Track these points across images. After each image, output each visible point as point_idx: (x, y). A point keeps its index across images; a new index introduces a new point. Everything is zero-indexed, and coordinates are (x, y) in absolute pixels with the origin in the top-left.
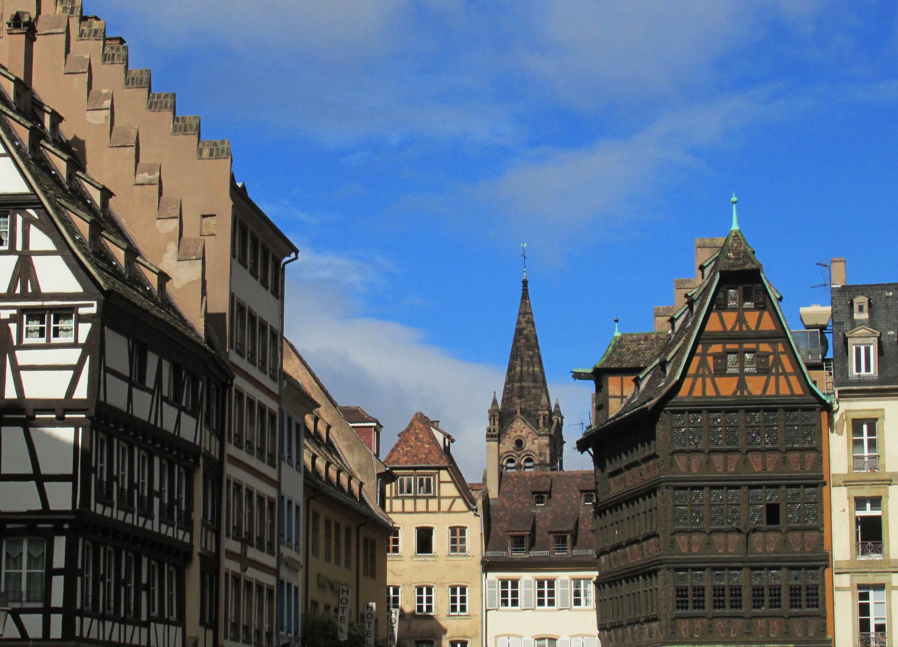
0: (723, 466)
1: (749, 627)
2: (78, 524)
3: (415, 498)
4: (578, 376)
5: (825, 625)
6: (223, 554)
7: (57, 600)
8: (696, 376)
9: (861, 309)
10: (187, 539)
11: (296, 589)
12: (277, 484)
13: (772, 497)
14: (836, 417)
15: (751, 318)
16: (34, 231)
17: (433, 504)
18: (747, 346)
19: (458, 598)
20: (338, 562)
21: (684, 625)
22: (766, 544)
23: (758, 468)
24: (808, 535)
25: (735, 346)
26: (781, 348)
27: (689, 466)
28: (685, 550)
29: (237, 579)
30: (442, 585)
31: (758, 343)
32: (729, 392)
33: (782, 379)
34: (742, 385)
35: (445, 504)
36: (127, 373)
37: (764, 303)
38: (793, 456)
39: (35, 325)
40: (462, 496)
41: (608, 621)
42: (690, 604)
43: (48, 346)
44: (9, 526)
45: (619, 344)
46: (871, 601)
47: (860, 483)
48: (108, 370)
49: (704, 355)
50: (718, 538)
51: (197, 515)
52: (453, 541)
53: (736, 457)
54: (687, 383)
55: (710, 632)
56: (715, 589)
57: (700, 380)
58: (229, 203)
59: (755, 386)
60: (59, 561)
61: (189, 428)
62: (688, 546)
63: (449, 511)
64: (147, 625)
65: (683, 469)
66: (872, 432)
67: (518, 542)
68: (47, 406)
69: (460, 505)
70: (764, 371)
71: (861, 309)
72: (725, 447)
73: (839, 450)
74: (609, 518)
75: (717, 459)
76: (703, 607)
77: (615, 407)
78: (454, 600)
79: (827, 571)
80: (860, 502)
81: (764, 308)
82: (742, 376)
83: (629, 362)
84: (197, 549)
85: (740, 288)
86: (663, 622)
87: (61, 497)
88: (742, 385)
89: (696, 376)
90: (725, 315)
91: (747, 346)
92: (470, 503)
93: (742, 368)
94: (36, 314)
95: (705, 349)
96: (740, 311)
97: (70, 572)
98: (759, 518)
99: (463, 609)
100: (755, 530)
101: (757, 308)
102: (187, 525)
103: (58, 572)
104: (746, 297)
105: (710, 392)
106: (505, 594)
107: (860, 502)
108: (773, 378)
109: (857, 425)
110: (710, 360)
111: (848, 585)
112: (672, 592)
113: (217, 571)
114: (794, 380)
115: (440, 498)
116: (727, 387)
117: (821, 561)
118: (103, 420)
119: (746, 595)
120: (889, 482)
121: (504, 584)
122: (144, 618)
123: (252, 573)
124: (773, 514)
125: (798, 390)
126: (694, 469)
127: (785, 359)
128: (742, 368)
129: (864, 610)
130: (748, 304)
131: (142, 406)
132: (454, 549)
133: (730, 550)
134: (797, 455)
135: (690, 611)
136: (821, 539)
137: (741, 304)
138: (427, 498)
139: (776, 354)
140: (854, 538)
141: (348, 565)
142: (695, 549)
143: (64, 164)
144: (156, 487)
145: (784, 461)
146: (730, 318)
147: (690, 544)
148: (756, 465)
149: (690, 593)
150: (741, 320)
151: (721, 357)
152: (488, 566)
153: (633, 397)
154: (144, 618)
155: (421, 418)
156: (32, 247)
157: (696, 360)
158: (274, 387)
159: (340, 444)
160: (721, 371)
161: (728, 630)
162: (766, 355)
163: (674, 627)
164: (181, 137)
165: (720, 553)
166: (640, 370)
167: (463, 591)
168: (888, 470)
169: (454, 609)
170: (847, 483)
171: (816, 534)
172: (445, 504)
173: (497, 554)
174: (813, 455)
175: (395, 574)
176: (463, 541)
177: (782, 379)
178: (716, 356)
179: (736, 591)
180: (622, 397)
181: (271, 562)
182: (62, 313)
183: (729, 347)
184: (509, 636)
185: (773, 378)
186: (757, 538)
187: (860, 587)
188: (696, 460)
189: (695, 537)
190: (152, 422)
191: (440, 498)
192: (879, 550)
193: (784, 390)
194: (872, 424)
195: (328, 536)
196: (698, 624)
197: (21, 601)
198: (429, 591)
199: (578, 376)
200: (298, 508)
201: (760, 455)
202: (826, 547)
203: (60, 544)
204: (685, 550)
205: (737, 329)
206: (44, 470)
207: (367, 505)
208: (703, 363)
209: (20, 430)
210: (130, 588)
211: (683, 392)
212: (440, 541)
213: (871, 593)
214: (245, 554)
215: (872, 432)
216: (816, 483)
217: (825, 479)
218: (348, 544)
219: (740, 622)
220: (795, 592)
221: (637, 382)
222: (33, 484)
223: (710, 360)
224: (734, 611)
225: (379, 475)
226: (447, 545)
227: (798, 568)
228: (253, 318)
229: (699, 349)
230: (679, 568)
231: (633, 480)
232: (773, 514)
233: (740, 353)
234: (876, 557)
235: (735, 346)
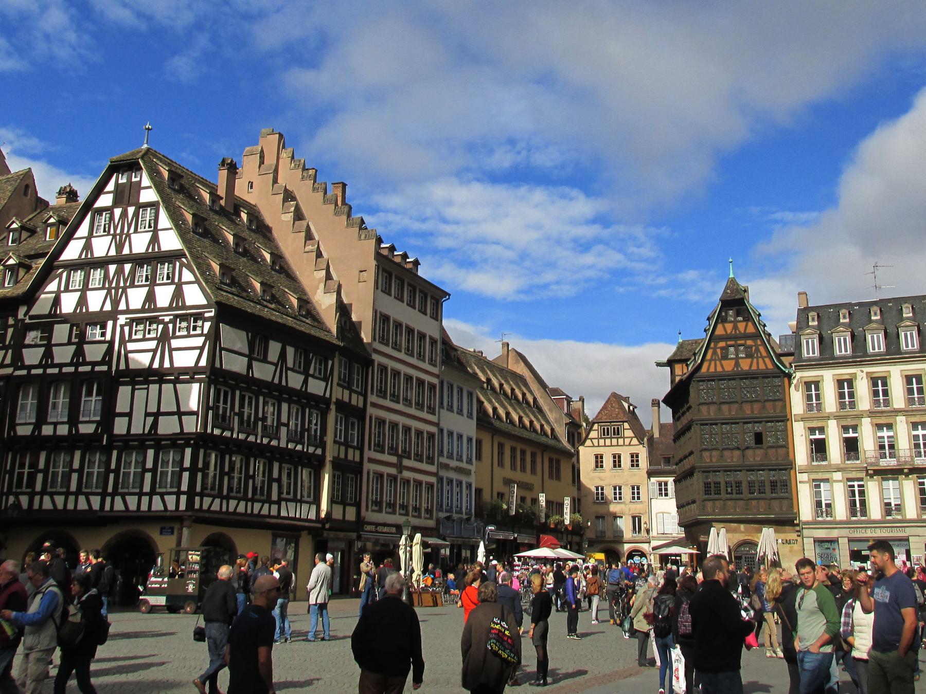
0: (727, 411)
2: (201, 441)
3: (611, 438)
4: (659, 364)
6: (365, 460)
7: (184, 487)
9: (813, 320)
10: (319, 451)
11: (469, 486)
12: (437, 425)
13: (758, 428)
14: (795, 381)
16: (184, 270)
17: (621, 441)
18: (739, 342)
19: (636, 491)
20: (523, 469)
21: (709, 504)
22: (755, 456)
23: (748, 412)
24: (779, 450)
25: (733, 343)
26: (759, 342)
27: (709, 412)
28: (708, 460)
29: (393, 478)
30: (627, 485)
32: (730, 369)
33: (760, 360)
34: (737, 364)
35: (627, 441)
37: (748, 318)
38: (768, 404)
39: (184, 324)
40: (636, 437)
41: (683, 501)
42: (713, 492)
43: (189, 336)
44: (163, 443)
46: (822, 489)
48: (221, 349)
49: (715, 349)
50: (727, 453)
51: (329, 438)
52: (632, 461)
53: (736, 405)
54: (705, 365)
55: (724, 508)
57: (713, 363)
58: (374, 263)
59: (745, 365)
60: (187, 464)
61: (316, 387)
62: (710, 459)
63: (630, 445)
65: (706, 414)
66: (817, 389)
67: (668, 461)
68: (184, 371)
69: (635, 441)
71: (813, 320)
72: (728, 400)
73: (797, 401)
74: (678, 443)
75: (725, 408)
78: (633, 493)
79: (792, 472)
80: (812, 430)
82: (737, 359)
83: (685, 355)
84: (329, 458)
85: (735, 308)
86: (698, 503)
87: (191, 426)
88: (737, 364)
89: (710, 360)
90: (727, 325)
91: (739, 342)
92: (641, 442)
93: (737, 355)
94: (184, 318)
95: (715, 345)
96: (735, 323)
97: (193, 470)
98: (750, 439)
99: (638, 498)
100: (747, 448)
101: (744, 320)
102: (323, 445)
103: (186, 470)
104: (738, 314)
105: (719, 369)
106: (660, 490)
107: (812, 430)
108: (755, 360)
109: (808, 385)
110: (719, 351)
111: (806, 479)
112: (701, 485)
113: (361, 472)
114: (767, 360)
115: (624, 438)
116: (729, 366)
117: (788, 465)
118: (215, 377)
119: (744, 487)
120: (828, 418)
121: (660, 485)
122: (275, 497)
123: (406, 474)
124: (758, 438)
125: (770, 366)
126: (712, 414)
127: (762, 349)
128: (737, 355)
129: (818, 494)
130: (740, 318)
131: (263, 372)
132: (632, 466)
134: (771, 403)
135: (713, 496)
136: (787, 454)
137: (735, 319)
138: (618, 438)
139: (757, 346)
140: (809, 452)
141: (533, 471)
142: (714, 460)
143: (232, 237)
144: (284, 419)
145: (764, 407)
146: (729, 327)
147: (711, 456)
148: (747, 410)
149: (712, 486)
151: (725, 349)
152: (650, 474)
154: (275, 497)
155: (614, 395)
156: (183, 280)
157: (710, 352)
158: (435, 370)
159: (546, 408)
160: (725, 357)
161: (735, 507)
162: (751, 347)
163: (704, 506)
164: (350, 230)
165: (728, 462)
166: (688, 360)
167: (638, 488)
168: (828, 410)
169: (633, 498)
170: (802, 420)
171: (784, 449)
172: (627, 441)
173: (656, 467)
174: (780, 403)
175: (601, 480)
176: (637, 461)
177: (760, 360)
178: (722, 349)
179: (738, 484)
181: (433, 469)
182: (198, 317)
183: (729, 343)
184: (663, 513)
185: (755, 360)
186: (749, 453)
187: (814, 480)
188: (713, 408)
189: (714, 453)
190: (276, 381)
191: (624, 438)
192: (825, 459)
193: (762, 366)
194: (817, 384)
195: (513, 457)
196: (718, 503)
197: (166, 487)
198: (620, 488)
199: (659, 364)
200: (470, 440)
201: (749, 404)
202: (791, 457)
203: (188, 451)
204: (708, 460)
206: (182, 410)
207: (559, 441)
208: (715, 353)
209: (171, 385)
210: (233, 477)
211: (704, 369)
212: (626, 461)
213: (822, 484)
214: (401, 463)
215: (817, 389)
216: (783, 419)
217: (789, 417)
218: (533, 462)
219: (741, 503)
220: (773, 485)
221: (687, 365)
222: (176, 417)
223: (719, 351)
224: (738, 496)
225: (566, 424)
226: (629, 463)
227: (775, 470)
228: (410, 331)
229: (712, 345)
230: (706, 471)
231: (684, 420)
232: (758, 438)
233: (736, 347)
234: (824, 463)
235: (733, 343)
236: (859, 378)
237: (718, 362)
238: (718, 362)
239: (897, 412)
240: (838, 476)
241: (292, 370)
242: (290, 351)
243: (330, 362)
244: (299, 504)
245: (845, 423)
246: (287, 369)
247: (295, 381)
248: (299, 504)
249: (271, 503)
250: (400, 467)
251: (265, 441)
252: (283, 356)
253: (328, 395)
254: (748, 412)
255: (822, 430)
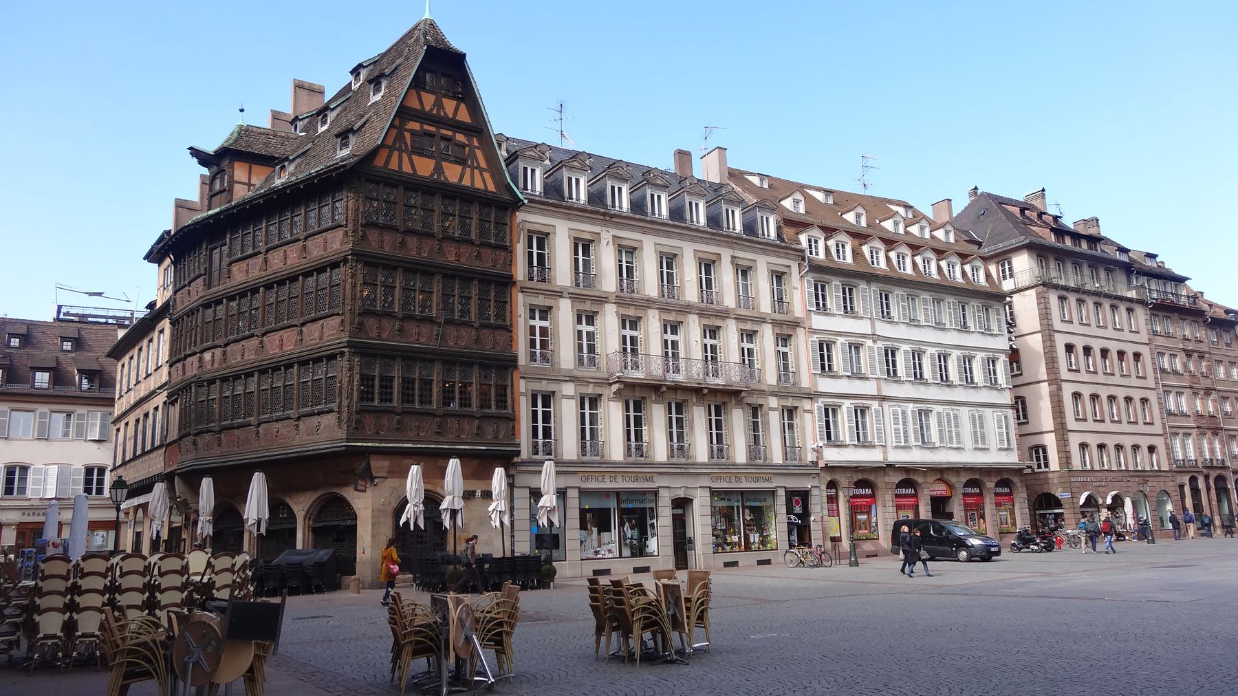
1: (439, 427)
4: (195, 152)
5: (514, 427)
8: (392, 149)
15: (449, 105)
21: (369, 420)
23: (452, 258)
26: (476, 143)
28: (374, 334)
31: (455, 132)
34: (438, 169)
45: (245, 132)
47: (536, 292)
54: (384, 154)
56: (403, 382)
57: (396, 154)
59: (452, 173)
70: (462, 161)
75: (412, 241)
76: (391, 400)
77: (241, 193)
79: (516, 375)
81: (462, 100)
88: (438, 169)
90: (424, 95)
101: (454, 98)
105: (407, 168)
108: (468, 170)
110: (408, 136)
114: (487, 175)
116: (424, 167)
120: (558, 294)
125: (491, 188)
127: (479, 153)
133: (422, 340)
139: (473, 148)
142: (385, 335)
146: (429, 100)
150: (439, 104)
153: (261, 187)
162: (463, 146)
170: (523, 290)
180: (249, 185)
183: (426, 127)
185: (468, 170)
189: (386, 323)
193: (479, 184)
199: (195, 152)
205: (435, 112)
211: (379, 162)
223: (408, 136)
235: (433, 129)
236: (604, 242)
237: (405, 156)
238: (405, 156)
239: (648, 303)
240: (569, 389)
245: (582, 307)
254: (452, 258)
255: (545, 313)
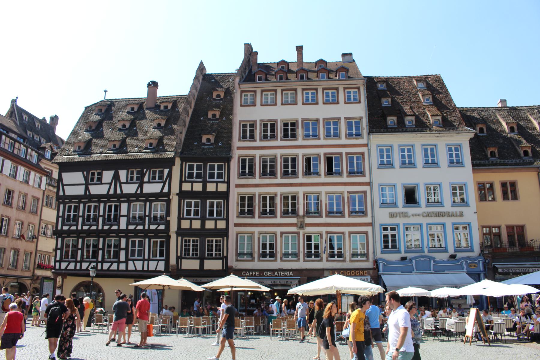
10: (162, 227)
36: (84, 182)
61: (150, 188)
64: (126, 262)
123: (309, 230)
190: (112, 192)
241: (127, 183)
242: (123, 174)
243: (166, 171)
244: (146, 262)
246: (121, 184)
247: (130, 189)
248: (146, 262)
249: (119, 262)
250: (302, 226)
251: (106, 227)
252: (116, 177)
253: (166, 190)
